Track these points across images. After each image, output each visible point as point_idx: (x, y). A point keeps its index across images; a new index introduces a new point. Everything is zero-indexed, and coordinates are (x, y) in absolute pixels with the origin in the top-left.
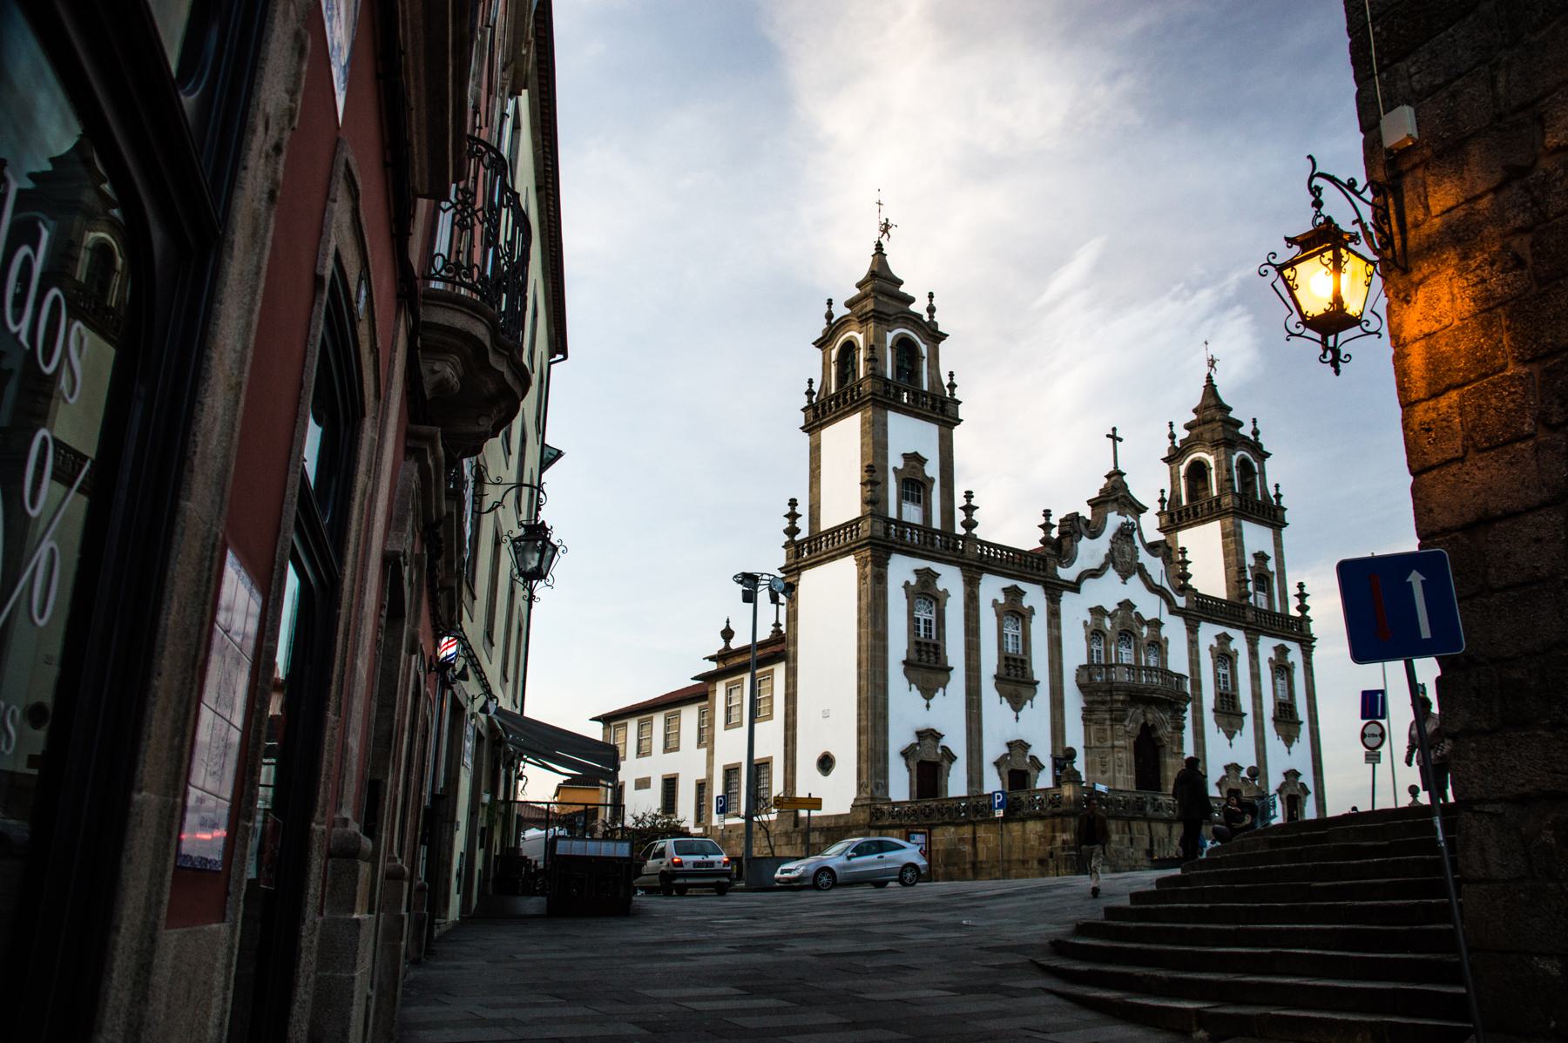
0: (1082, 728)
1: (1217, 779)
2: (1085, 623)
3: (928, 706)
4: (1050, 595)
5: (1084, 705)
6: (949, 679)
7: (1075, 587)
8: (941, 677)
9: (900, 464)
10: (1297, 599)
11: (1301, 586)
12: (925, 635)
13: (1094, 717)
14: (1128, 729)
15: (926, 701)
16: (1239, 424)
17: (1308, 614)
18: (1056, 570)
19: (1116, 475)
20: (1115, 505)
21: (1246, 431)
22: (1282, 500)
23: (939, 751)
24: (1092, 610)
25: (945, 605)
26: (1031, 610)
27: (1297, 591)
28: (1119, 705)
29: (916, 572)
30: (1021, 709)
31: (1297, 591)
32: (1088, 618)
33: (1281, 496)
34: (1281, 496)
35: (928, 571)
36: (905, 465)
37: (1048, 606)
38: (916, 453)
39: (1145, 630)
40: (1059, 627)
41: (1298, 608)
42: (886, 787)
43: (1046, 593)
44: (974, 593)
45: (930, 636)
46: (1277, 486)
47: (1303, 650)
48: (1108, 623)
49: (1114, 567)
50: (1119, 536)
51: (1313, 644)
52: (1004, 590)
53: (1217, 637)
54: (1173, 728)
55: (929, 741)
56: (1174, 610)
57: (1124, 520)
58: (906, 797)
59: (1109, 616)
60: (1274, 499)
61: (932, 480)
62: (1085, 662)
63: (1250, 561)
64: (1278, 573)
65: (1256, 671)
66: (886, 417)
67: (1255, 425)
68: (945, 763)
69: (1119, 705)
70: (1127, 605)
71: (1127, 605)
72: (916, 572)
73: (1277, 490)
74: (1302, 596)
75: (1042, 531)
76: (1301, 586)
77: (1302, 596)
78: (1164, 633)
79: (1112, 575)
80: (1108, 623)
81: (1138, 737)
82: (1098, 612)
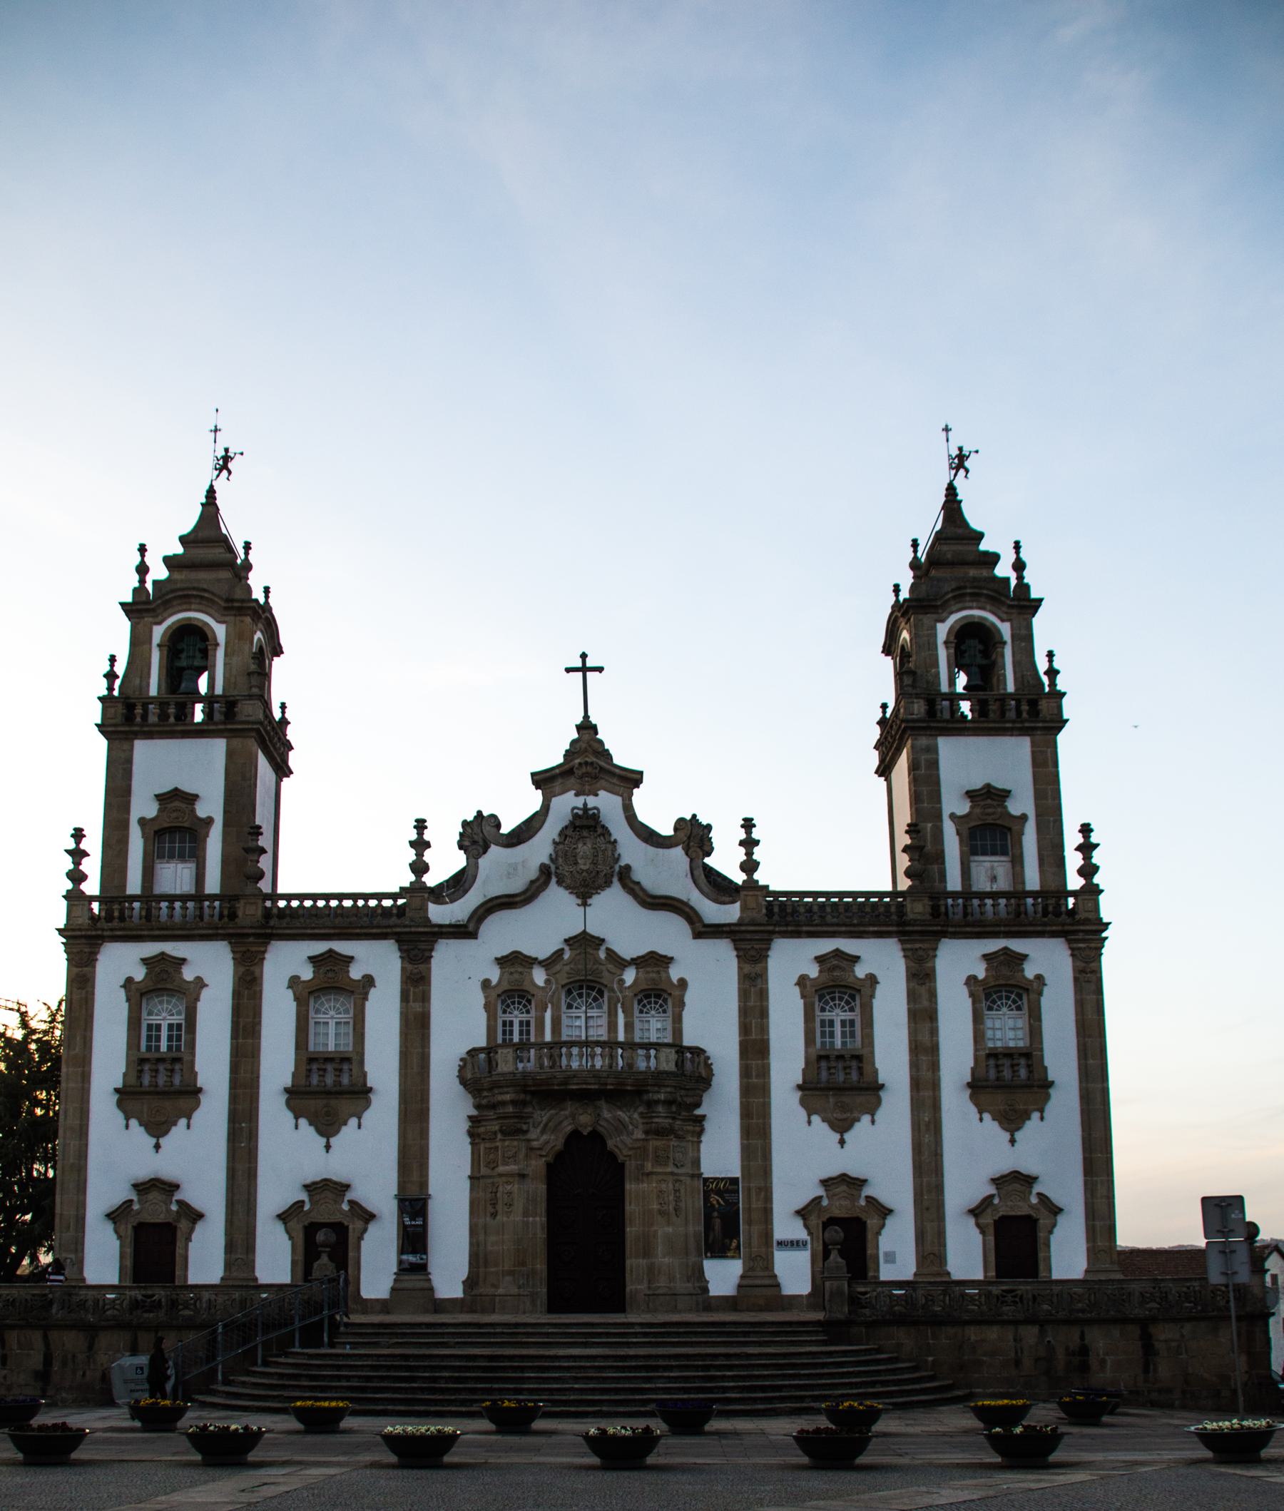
0: (469, 1148)
1: (802, 1200)
2: (486, 984)
3: (157, 1147)
4: (406, 951)
5: (474, 1112)
6: (198, 1104)
7: (465, 931)
8: (183, 1103)
9: (151, 810)
10: (1079, 855)
11: (1086, 830)
12: (170, 1048)
13: (482, 1130)
14: (535, 1144)
15: (154, 1141)
16: (993, 559)
17: (1096, 880)
18: (426, 910)
19: (587, 728)
20: (572, 780)
21: (1004, 570)
23: (174, 1207)
24: (502, 962)
25: (197, 999)
26: (369, 981)
27: (1079, 839)
28: (510, 1109)
29: (145, 961)
30: (337, 1132)
31: (1079, 839)
32: (494, 975)
33: (1057, 672)
34: (1057, 672)
35: (163, 956)
36: (160, 811)
37: (403, 969)
38: (176, 789)
40: (425, 998)
41: (1081, 872)
42: (80, 1263)
43: (400, 950)
44: (253, 973)
45: (158, 1048)
46: (1050, 655)
47: (1072, 949)
48: (539, 977)
49: (559, 883)
50: (569, 832)
51: (1104, 935)
52: (312, 959)
53: (820, 959)
54: (647, 1132)
55: (154, 1196)
56: (703, 930)
57: (579, 801)
58: (112, 1278)
60: (1045, 680)
61: (209, 821)
62: (482, 1043)
63: (954, 804)
64: (1038, 816)
65: (925, 1003)
66: (132, 750)
67: (1017, 553)
68: (183, 1225)
69: (510, 1109)
70: (584, 942)
71: (584, 942)
72: (145, 961)
73: (1051, 661)
74: (1087, 848)
75: (413, 852)
76: (1086, 830)
77: (1087, 848)
78: (675, 973)
79: (558, 899)
80: (539, 977)
81: (559, 1156)
82: (514, 962)
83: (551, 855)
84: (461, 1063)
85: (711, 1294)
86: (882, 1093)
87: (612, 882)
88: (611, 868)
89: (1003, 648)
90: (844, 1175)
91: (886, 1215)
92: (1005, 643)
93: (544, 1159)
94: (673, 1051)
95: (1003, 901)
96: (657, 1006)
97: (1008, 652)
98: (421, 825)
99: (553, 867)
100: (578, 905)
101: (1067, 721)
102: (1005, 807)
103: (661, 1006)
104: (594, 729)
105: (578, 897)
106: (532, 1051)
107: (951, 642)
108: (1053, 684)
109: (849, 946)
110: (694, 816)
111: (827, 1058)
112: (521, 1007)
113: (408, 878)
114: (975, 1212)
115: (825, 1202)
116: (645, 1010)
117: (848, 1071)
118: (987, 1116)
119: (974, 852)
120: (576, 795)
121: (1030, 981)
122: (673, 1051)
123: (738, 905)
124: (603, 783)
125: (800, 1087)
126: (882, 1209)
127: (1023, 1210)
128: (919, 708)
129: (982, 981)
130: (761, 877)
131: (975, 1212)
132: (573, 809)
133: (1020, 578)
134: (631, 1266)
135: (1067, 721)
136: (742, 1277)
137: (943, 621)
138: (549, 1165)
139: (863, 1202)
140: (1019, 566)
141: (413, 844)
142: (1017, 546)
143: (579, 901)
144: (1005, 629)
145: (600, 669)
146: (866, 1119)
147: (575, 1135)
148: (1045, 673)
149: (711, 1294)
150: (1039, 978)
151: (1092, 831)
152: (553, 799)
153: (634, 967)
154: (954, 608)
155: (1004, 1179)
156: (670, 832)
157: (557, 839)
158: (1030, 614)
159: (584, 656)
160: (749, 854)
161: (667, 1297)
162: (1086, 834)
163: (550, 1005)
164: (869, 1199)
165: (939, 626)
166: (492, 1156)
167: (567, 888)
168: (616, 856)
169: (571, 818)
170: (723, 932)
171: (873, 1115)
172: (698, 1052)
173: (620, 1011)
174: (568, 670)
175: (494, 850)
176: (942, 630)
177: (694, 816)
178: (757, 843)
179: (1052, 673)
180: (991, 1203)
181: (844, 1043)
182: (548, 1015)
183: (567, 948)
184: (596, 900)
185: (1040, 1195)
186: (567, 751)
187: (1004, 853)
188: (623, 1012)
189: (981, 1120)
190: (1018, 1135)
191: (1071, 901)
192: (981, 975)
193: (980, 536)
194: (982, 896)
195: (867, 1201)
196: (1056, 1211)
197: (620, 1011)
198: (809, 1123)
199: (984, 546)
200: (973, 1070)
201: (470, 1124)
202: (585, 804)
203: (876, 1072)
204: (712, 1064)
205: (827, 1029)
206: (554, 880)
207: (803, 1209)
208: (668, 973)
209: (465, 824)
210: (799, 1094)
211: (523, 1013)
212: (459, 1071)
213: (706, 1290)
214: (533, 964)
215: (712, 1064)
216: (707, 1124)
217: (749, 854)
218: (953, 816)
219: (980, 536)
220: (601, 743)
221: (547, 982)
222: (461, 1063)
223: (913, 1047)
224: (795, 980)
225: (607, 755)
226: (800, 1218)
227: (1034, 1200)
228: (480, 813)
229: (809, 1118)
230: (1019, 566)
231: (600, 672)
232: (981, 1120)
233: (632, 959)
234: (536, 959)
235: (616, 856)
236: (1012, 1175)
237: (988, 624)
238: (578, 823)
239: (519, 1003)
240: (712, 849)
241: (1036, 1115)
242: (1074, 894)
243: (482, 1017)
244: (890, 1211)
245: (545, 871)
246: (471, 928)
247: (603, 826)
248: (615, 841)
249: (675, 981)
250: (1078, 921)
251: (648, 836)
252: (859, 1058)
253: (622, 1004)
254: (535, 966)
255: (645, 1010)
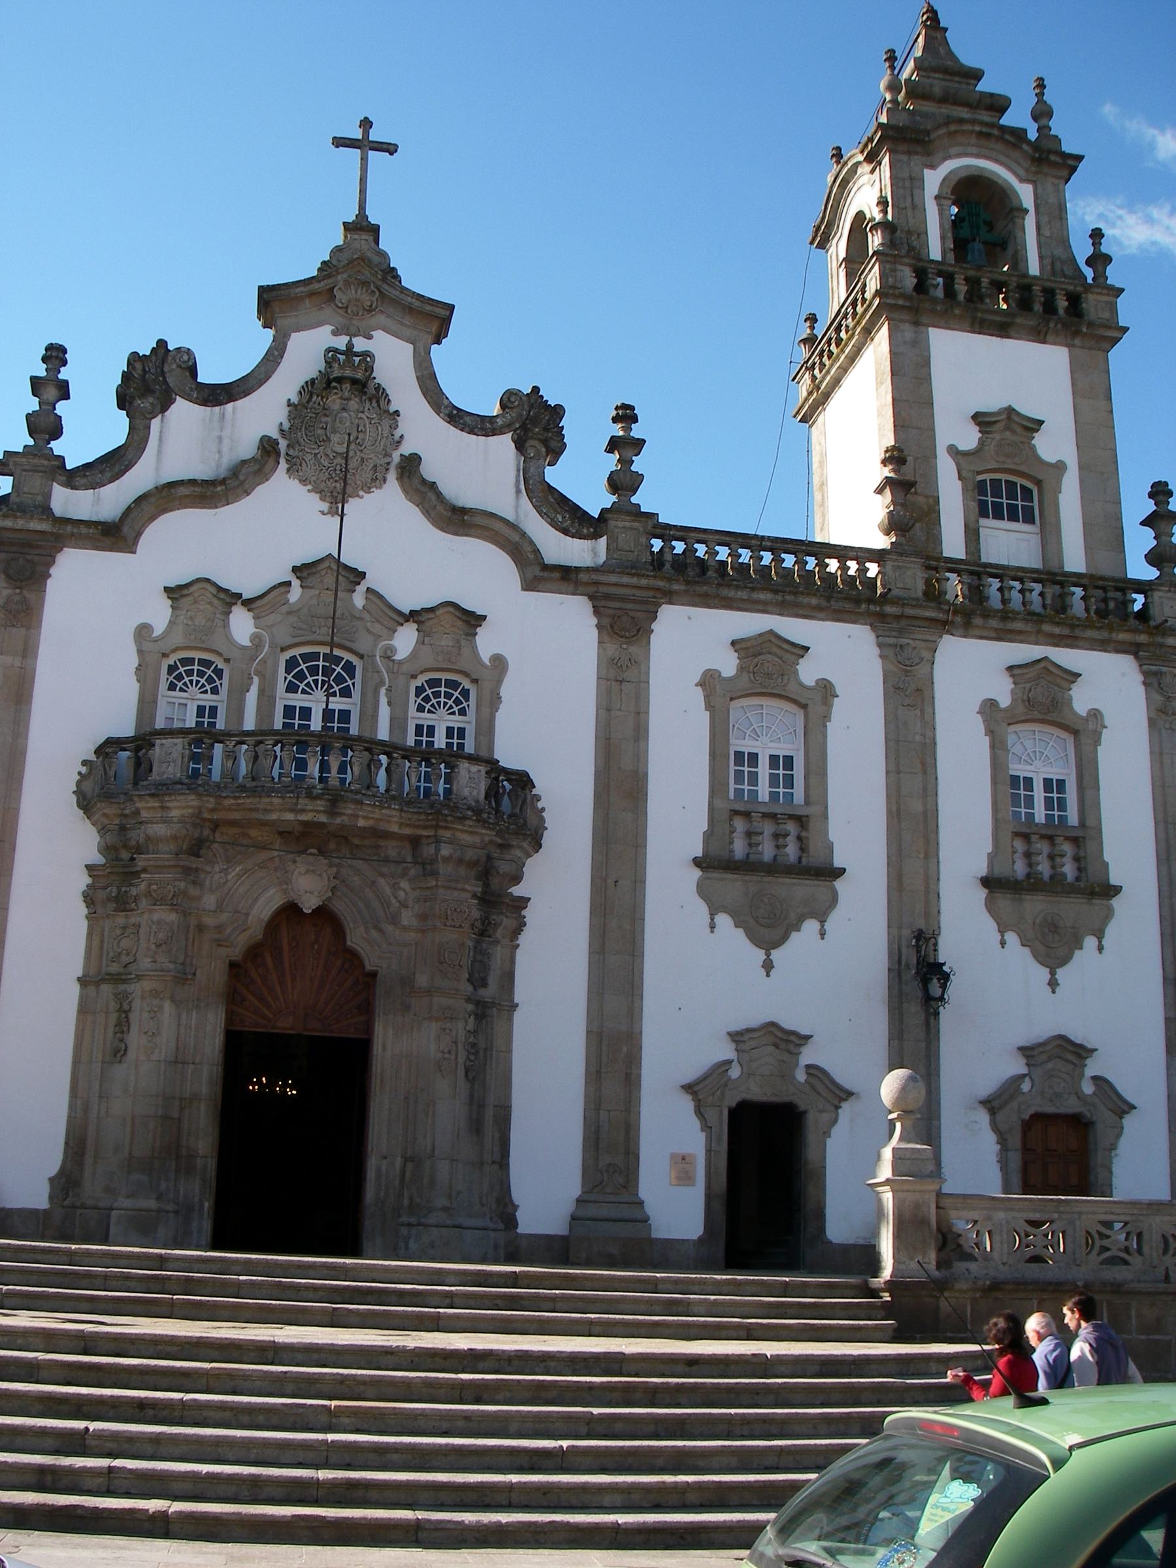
0: (84, 925)
1: (694, 1066)
2: (142, 632)
5: (97, 859)
10: (1149, 533)
22: (1110, 270)
24: (175, 593)
27: (1150, 507)
31: (1150, 507)
32: (159, 615)
33: (1108, 259)
34: (1108, 259)
39: (405, 640)
47: (1145, 674)
48: (242, 626)
49: (293, 469)
57: (341, 342)
59: (248, 603)
60: (1089, 273)
78: (487, 643)
83: (281, 424)
84: (84, 770)
85: (519, 1231)
86: (839, 884)
87: (385, 481)
88: (389, 455)
89: (1024, 219)
90: (773, 1024)
91: (842, 1100)
92: (1026, 211)
93: (223, 951)
94: (483, 769)
95: (1038, 587)
96: (450, 702)
97: (1030, 223)
98: (55, 355)
99: (283, 444)
100: (323, 513)
101: (1125, 330)
102: (1033, 449)
103: (457, 702)
104: (375, 230)
105: (322, 499)
106: (218, 748)
107: (945, 198)
108: (1100, 276)
109: (793, 628)
110: (536, 389)
111: (746, 815)
112: (203, 681)
113: (20, 439)
114: (992, 1104)
115: (735, 1072)
116: (428, 706)
117: (781, 841)
118: (1012, 938)
119: (984, 513)
120: (335, 333)
121: (1081, 718)
122: (483, 769)
123: (603, 541)
124: (381, 319)
125: (697, 862)
126: (838, 1092)
127: (1070, 1106)
128: (909, 280)
129: (1006, 710)
130: (644, 499)
131: (992, 1104)
132: (329, 350)
133: (1043, 130)
134: (379, 1170)
135: (1125, 330)
136: (579, 1201)
137: (933, 167)
138: (233, 965)
139: (801, 1076)
140: (1042, 113)
141: (37, 385)
142: (1041, 84)
143: (325, 506)
144: (1025, 194)
145: (391, 149)
146: (811, 926)
147: (291, 910)
148: (1089, 262)
149: (521, 1230)
150: (1095, 714)
151: (1170, 494)
152: (293, 335)
153: (415, 626)
154: (953, 151)
155: (1041, 1049)
156: (495, 410)
157: (295, 399)
158: (1060, 178)
159: (366, 124)
160: (625, 462)
161: (444, 1230)
162: (1161, 498)
163: (256, 680)
164: (812, 1071)
165: (927, 172)
166: (125, 943)
167: (304, 481)
168: (397, 437)
169: (322, 365)
170: (577, 583)
171: (822, 922)
172: (522, 781)
173: (383, 700)
174: (339, 142)
175: (182, 409)
176: (933, 180)
177: (536, 389)
178: (639, 444)
179: (1099, 260)
180: (1018, 1090)
181: (774, 796)
182: (252, 697)
183: (296, 583)
184: (352, 506)
185: (1096, 1079)
186: (324, 263)
187: (1028, 519)
188: (389, 704)
189: (1003, 943)
190: (1061, 973)
191: (1139, 600)
192: (1005, 701)
193: (977, 75)
194: (1001, 572)
195: (808, 1074)
196: (1123, 1108)
197: (383, 700)
198: (712, 927)
199: (983, 86)
200: (992, 858)
201: (89, 880)
202: (350, 346)
203: (830, 847)
204: (543, 809)
205: (746, 769)
206: (283, 465)
207: (698, 1082)
208: (474, 648)
209: (134, 358)
210: (697, 873)
211: (206, 692)
212: (78, 784)
213: (510, 1221)
214: (231, 605)
215: (543, 809)
216: (529, 913)
217: (625, 462)
218: (953, 451)
219: (977, 75)
220: (384, 255)
221: (257, 640)
222: (84, 770)
223: (894, 808)
224: (697, 679)
225: (391, 274)
226: (690, 1097)
227: (1088, 1088)
228: (162, 343)
229: (712, 920)
230: (1042, 113)
231: (391, 154)
232: (1003, 943)
233: (413, 613)
234: (239, 596)
235: (397, 437)
236: (1056, 1043)
237: (1000, 182)
238: (336, 373)
239: (201, 674)
240: (564, 446)
241: (1090, 942)
242: (1142, 587)
243: (130, 690)
244: (850, 1094)
245: (268, 448)
246: (125, 529)
247: (378, 387)
248: (397, 413)
249: (487, 662)
250: (1157, 627)
251: (457, 417)
252: (801, 821)
253: (389, 690)
254: (234, 609)
255: (428, 706)
